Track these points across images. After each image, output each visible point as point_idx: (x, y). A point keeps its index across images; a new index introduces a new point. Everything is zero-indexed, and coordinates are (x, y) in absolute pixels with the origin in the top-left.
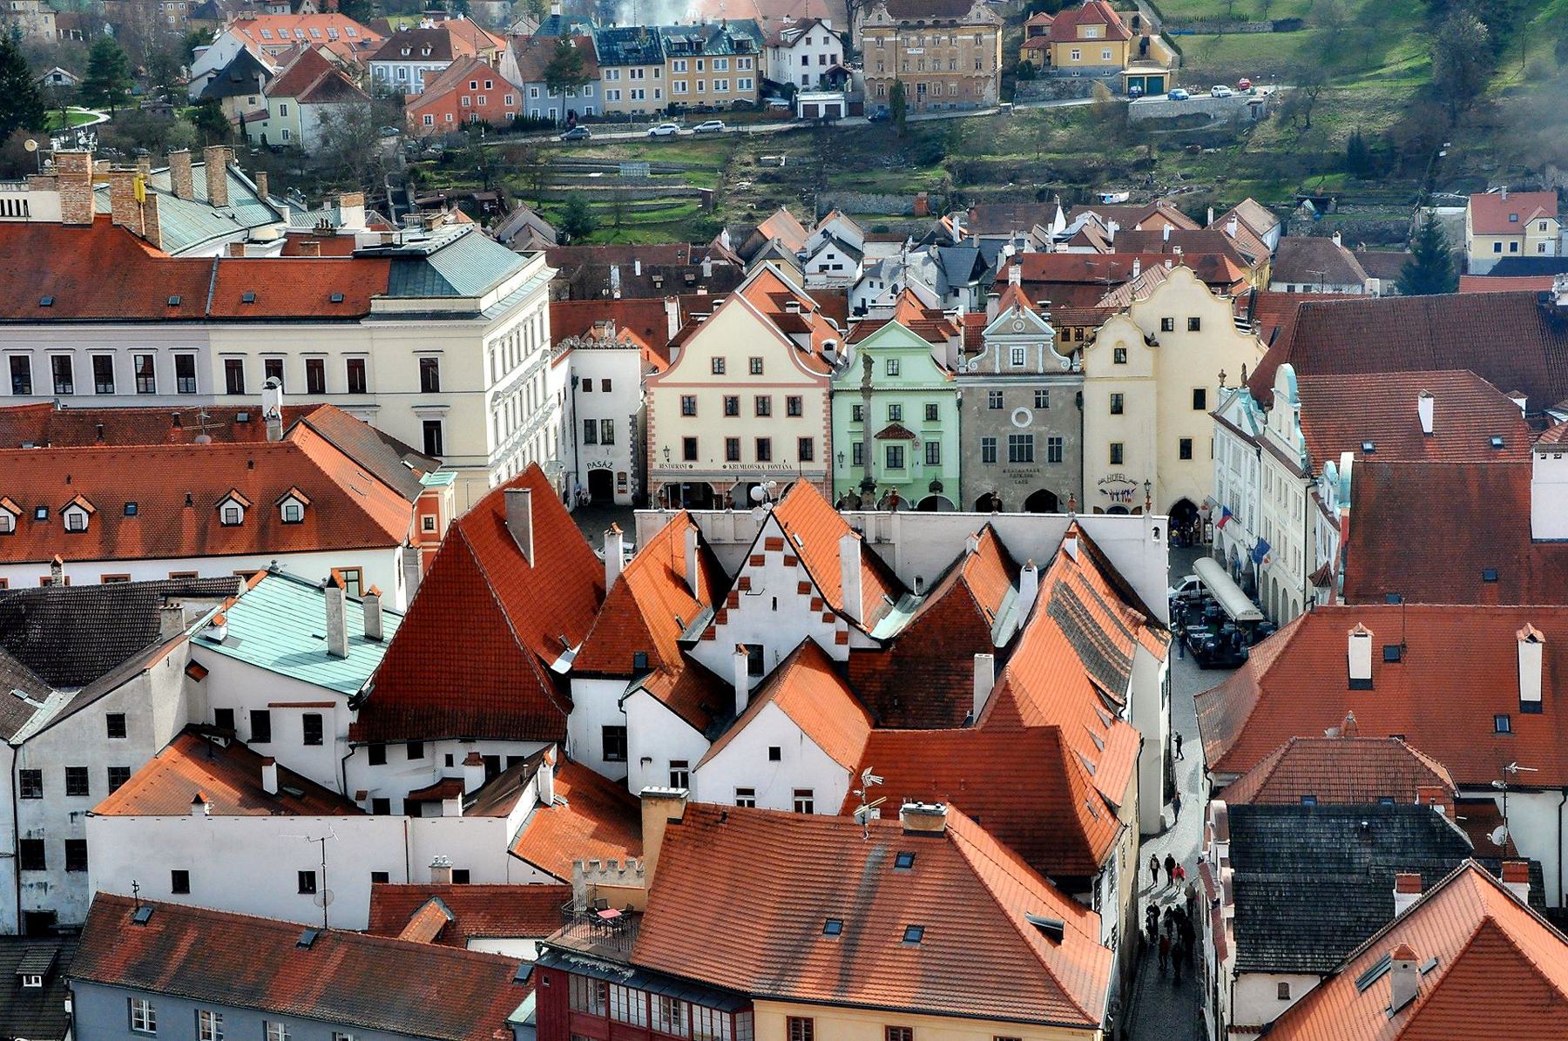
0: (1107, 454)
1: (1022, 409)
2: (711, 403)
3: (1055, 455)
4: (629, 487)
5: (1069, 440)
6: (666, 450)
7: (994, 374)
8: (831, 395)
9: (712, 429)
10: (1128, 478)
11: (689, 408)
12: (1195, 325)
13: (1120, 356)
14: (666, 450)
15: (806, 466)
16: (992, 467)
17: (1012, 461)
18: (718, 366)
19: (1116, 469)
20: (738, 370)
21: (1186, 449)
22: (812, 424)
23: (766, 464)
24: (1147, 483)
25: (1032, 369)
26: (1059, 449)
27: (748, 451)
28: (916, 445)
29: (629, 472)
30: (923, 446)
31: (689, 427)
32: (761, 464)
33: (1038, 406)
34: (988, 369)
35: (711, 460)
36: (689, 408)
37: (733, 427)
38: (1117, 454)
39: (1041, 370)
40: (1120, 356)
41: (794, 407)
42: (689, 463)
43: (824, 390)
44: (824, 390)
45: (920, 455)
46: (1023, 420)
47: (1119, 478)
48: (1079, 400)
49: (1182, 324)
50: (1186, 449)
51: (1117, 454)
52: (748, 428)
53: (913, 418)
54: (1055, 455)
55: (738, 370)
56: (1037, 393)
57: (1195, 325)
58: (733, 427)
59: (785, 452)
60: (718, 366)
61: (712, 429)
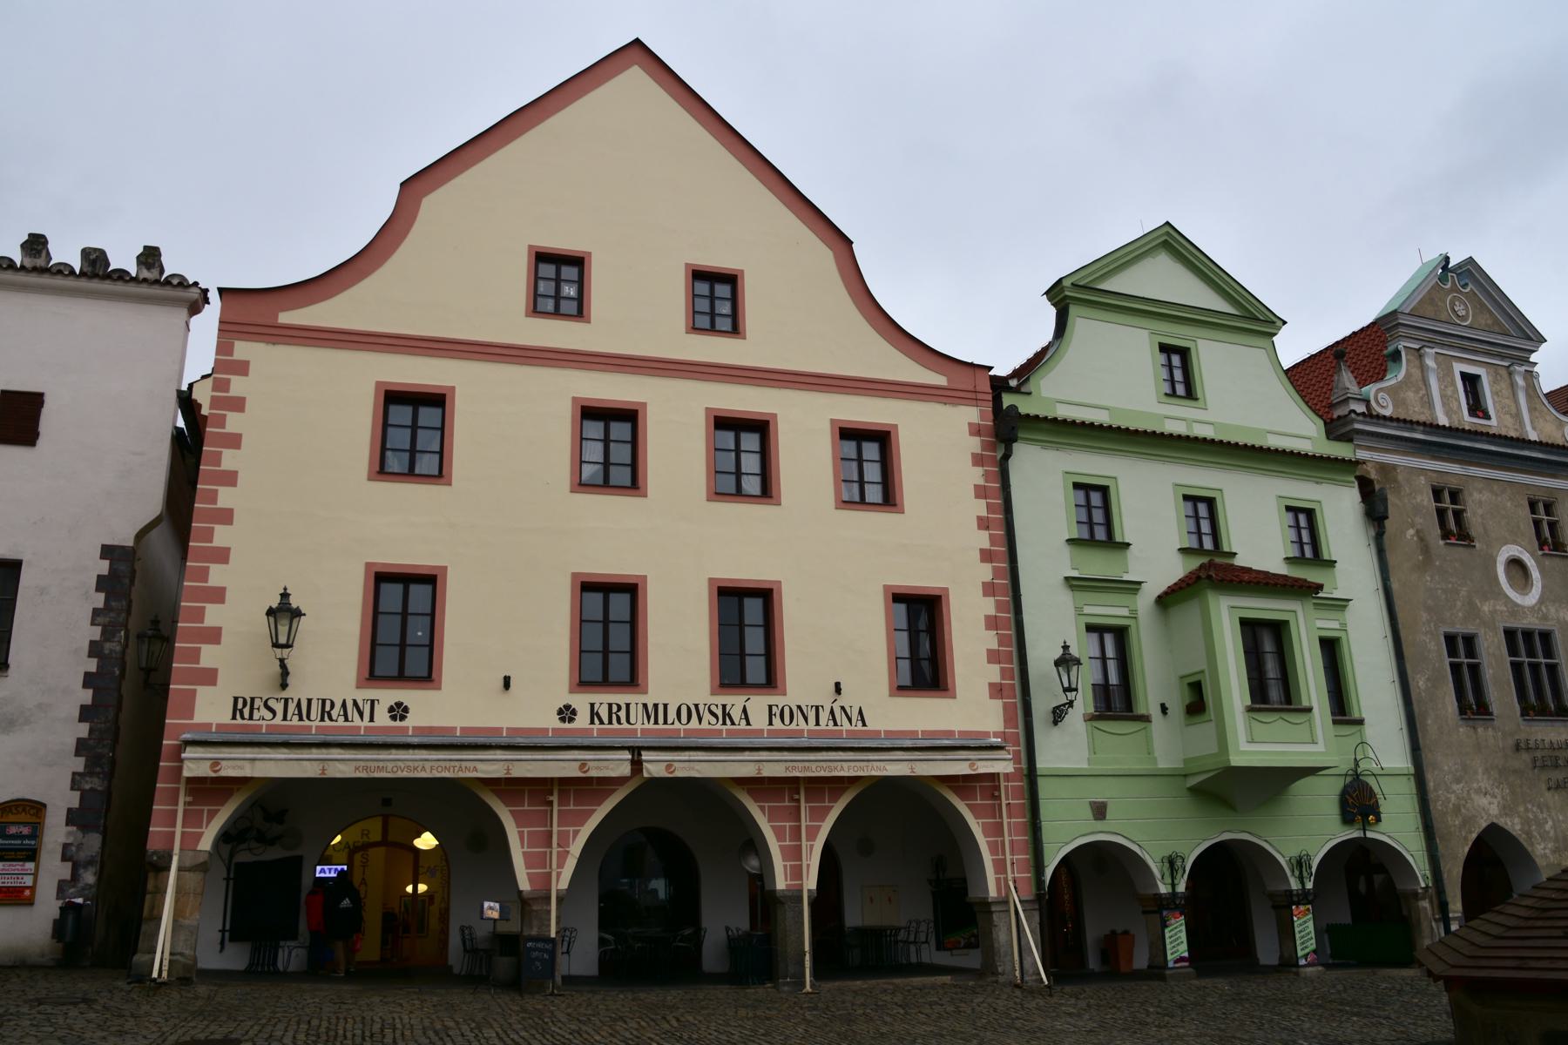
4: (52, 869)
6: (285, 612)
7: (1433, 427)
9: (510, 537)
11: (412, 432)
14: (285, 612)
15: (924, 714)
16: (1485, 733)
18: (559, 278)
20: (637, 306)
22: (936, 532)
23: (758, 705)
29: (60, 799)
31: (406, 526)
32: (735, 702)
33: (1542, 544)
35: (503, 680)
36: (412, 432)
37: (611, 536)
39: (1533, 436)
42: (387, 696)
43: (971, 414)
44: (971, 414)
52: (677, 542)
53: (1258, 540)
55: (637, 306)
56: (1533, 506)
59: (836, 655)
60: (559, 278)
61: (510, 537)
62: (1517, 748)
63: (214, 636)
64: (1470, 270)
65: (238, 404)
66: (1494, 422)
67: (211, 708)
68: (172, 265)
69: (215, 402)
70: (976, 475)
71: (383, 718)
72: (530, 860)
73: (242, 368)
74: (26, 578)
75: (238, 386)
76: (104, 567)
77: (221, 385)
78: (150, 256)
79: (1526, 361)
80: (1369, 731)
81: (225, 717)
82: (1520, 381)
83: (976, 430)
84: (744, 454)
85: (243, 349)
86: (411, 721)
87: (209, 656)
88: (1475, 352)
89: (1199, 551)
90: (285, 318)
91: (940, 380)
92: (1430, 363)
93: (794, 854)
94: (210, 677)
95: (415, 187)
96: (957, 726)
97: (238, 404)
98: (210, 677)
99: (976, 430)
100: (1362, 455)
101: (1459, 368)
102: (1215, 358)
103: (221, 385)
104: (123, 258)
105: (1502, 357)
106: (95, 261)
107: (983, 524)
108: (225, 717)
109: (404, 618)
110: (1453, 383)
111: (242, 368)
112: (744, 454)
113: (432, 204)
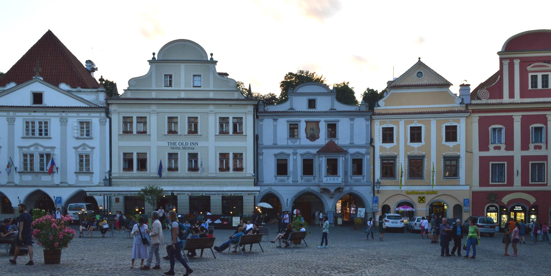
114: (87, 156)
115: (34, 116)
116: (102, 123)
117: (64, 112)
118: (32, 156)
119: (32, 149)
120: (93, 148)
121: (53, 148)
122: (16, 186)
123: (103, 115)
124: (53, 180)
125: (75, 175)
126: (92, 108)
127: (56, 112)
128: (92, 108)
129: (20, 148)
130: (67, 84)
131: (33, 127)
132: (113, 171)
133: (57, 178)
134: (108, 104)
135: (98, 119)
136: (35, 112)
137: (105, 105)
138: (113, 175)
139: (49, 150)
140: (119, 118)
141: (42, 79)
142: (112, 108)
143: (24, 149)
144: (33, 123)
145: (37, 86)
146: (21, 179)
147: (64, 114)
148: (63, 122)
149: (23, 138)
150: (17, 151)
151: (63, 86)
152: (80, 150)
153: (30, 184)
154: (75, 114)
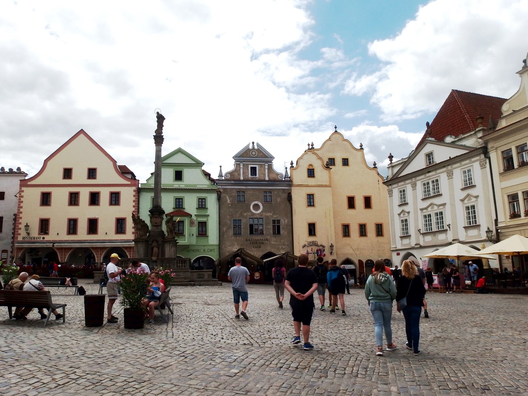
0: (305, 230)
1: (256, 202)
2: (59, 197)
3: (277, 230)
5: (284, 222)
6: (27, 226)
8: (139, 191)
10: (319, 244)
11: (46, 199)
12: (345, 162)
13: (311, 173)
14: (27, 226)
17: (251, 232)
18: (68, 173)
19: (312, 239)
20: (80, 176)
21: (346, 230)
24: (332, 246)
25: (263, 178)
26: (279, 227)
27: (83, 226)
28: (192, 223)
30: (196, 223)
31: (45, 212)
33: (266, 201)
34: (236, 178)
35: (58, 233)
36: (46, 199)
37: (73, 212)
38: (312, 229)
39: (267, 179)
40: (311, 173)
41: (115, 199)
42: (42, 236)
43: (134, 188)
44: (134, 188)
45: (195, 230)
46: (257, 209)
47: (314, 244)
48: (289, 198)
49: (339, 162)
50: (346, 230)
51: (312, 229)
52: (84, 212)
54: (277, 230)
55: (80, 176)
57: (345, 162)
58: (73, 212)
60: (68, 173)
62: (247, 240)
63: (20, 229)
64: (258, 145)
65: (22, 197)
66: (257, 176)
67: (20, 238)
68: (23, 170)
69: (20, 197)
70: (134, 199)
71: (41, 239)
72: (61, 258)
73: (23, 191)
74: (4, 219)
75: (22, 194)
76: (14, 217)
77: (20, 194)
78: (19, 169)
79: (271, 162)
80: (209, 238)
81: (21, 239)
82: (266, 167)
83: (134, 191)
84: (94, 199)
85: (23, 189)
86: (45, 239)
87: (20, 232)
88: (256, 162)
89: (179, 207)
90: (29, 183)
91: (129, 183)
92: (242, 166)
93: (98, 257)
94: (20, 234)
95: (46, 161)
96: (126, 239)
97: (22, 197)
98: (20, 234)
99: (134, 191)
100: (218, 187)
101: (250, 166)
102: (187, 173)
103: (20, 194)
104: (15, 170)
105: (263, 162)
106: (11, 170)
107: (134, 206)
108: (21, 239)
109: (44, 225)
110: (248, 169)
111: (23, 191)
112: (94, 199)
113: (49, 163)
114: (473, 207)
115: (428, 177)
116: (483, 166)
117: (449, 165)
118: (430, 216)
119: (429, 209)
120: (477, 197)
121: (444, 205)
122: (421, 247)
123: (483, 156)
124: (447, 238)
125: (464, 229)
126: (472, 153)
127: (444, 167)
128: (472, 153)
129: (422, 210)
130: (451, 134)
131: (428, 187)
132: (499, 221)
133: (449, 236)
134: (486, 143)
135: (478, 163)
136: (429, 172)
137: (484, 145)
138: (499, 225)
139: (442, 207)
140: (497, 154)
141: (433, 139)
142: (490, 146)
143: (424, 211)
144: (428, 183)
145: (429, 148)
146: (424, 240)
147: (449, 168)
148: (450, 175)
149: (423, 200)
150: (419, 211)
151: (449, 139)
152: (466, 201)
153: (431, 245)
154: (458, 165)
